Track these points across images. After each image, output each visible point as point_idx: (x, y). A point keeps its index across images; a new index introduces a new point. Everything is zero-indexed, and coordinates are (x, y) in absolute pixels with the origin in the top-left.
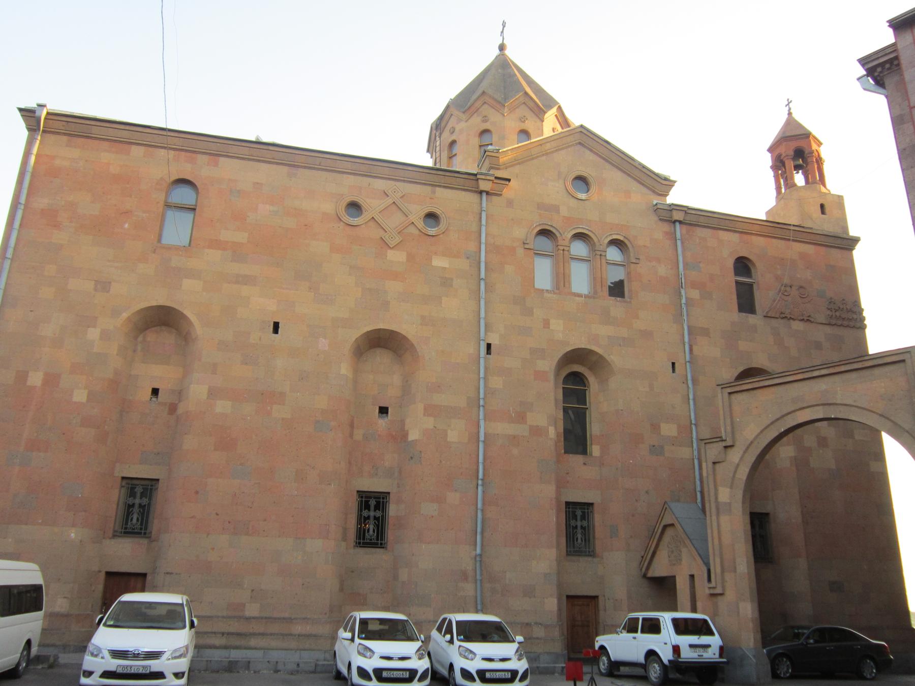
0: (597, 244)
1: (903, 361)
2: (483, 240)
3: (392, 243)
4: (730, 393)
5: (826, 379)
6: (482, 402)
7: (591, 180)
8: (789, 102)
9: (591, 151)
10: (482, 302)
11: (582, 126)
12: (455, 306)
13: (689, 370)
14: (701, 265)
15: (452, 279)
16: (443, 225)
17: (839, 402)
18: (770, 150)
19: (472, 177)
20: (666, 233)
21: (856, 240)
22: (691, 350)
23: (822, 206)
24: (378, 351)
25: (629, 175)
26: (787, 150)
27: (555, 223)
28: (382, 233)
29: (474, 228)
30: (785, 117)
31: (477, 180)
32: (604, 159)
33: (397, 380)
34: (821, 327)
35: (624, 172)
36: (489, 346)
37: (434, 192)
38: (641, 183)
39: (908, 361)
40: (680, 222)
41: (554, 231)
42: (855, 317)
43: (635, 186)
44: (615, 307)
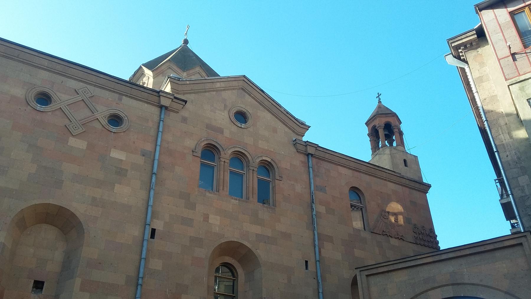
0: (251, 161)
1: (521, 244)
2: (159, 143)
3: (75, 133)
4: (367, 276)
5: (453, 262)
6: (140, 281)
7: (248, 115)
8: (379, 95)
9: (250, 95)
10: (152, 193)
11: (244, 76)
12: (128, 193)
13: (318, 267)
14: (327, 188)
15: (127, 170)
16: (124, 126)
17: (466, 281)
18: (367, 124)
19: (155, 93)
20: (302, 162)
21: (429, 186)
22: (320, 252)
23: (405, 161)
24: (45, 226)
25: (276, 117)
26: (380, 122)
27: (220, 140)
28: (67, 122)
29: (153, 132)
30: (377, 104)
31: (159, 96)
32: (259, 103)
33: (58, 256)
34: (410, 244)
35: (273, 114)
36: (153, 231)
37: (120, 99)
38: (284, 124)
39: (525, 244)
40: (312, 155)
41: (218, 146)
42: (432, 240)
43: (280, 126)
44: (263, 212)
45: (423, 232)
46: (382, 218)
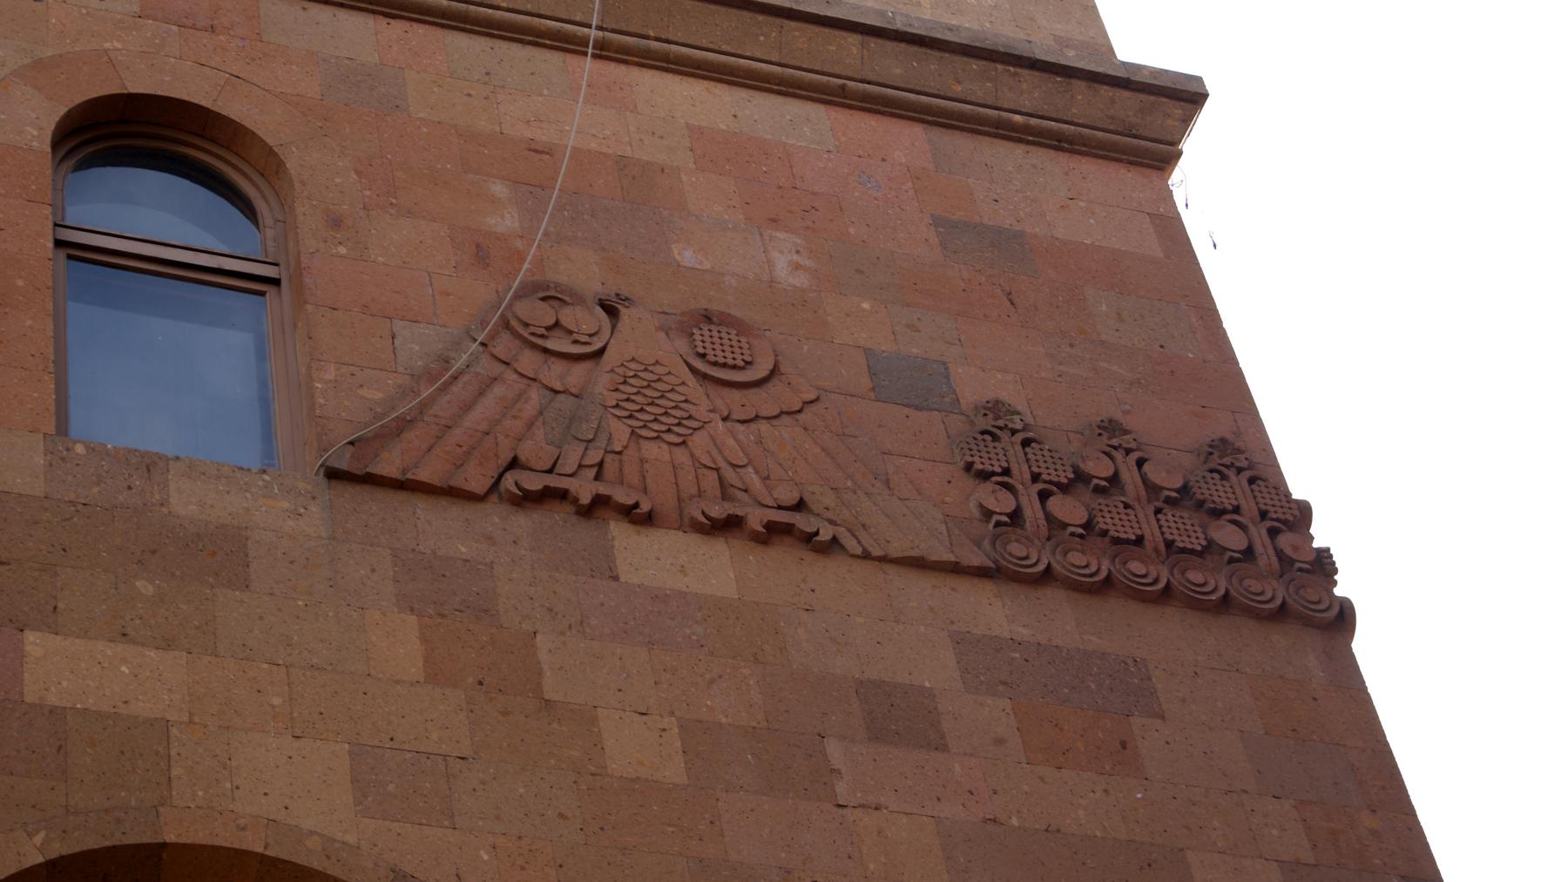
21: (1184, 97)
34: (919, 590)
42: (1229, 537)
45: (1100, 468)
46: (528, 361)
